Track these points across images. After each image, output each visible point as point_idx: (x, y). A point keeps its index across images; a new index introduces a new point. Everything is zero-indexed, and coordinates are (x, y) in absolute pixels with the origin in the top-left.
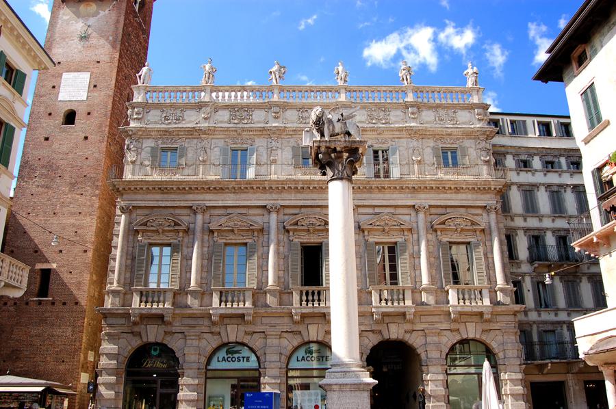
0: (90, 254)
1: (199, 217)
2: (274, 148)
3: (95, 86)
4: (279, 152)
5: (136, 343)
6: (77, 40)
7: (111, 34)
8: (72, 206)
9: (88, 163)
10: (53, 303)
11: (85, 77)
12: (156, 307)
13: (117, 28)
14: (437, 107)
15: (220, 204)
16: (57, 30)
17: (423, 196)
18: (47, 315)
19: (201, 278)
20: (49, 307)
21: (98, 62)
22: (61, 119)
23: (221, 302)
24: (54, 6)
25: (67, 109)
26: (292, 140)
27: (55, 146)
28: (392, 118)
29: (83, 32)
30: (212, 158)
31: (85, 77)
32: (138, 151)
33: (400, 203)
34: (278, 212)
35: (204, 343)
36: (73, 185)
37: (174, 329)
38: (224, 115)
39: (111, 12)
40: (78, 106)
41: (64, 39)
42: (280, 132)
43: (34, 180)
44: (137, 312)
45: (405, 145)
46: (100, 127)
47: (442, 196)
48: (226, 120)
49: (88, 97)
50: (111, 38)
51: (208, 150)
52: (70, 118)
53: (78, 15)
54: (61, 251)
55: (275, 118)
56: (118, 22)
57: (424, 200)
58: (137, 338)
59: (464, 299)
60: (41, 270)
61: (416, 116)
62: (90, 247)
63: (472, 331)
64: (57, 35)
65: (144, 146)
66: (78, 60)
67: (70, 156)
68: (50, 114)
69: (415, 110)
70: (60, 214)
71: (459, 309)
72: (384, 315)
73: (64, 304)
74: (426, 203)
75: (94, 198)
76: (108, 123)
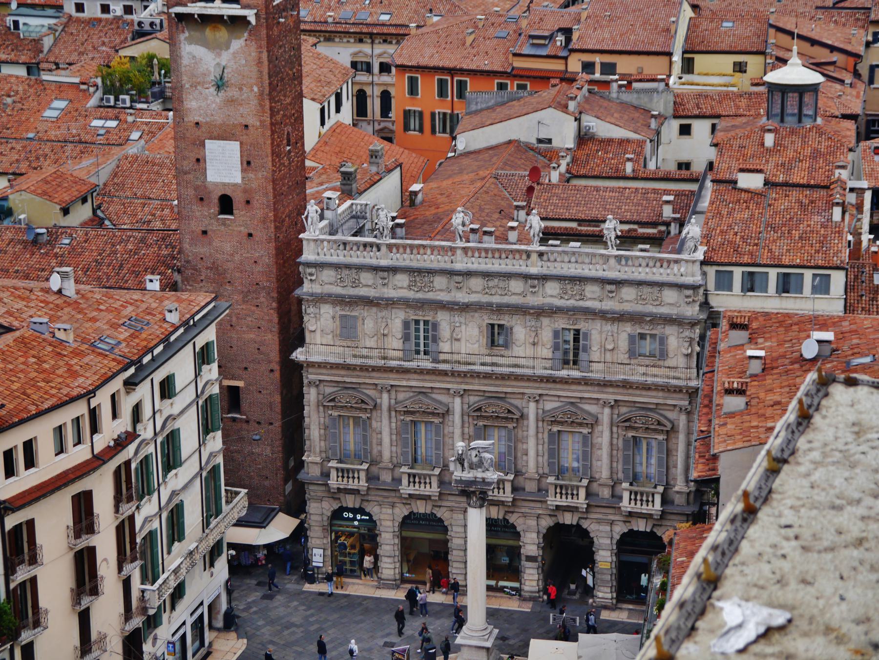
0: (277, 375)
1: (385, 396)
2: (458, 324)
3: (249, 163)
4: (463, 327)
5: (336, 506)
6: (212, 90)
7: (253, 81)
8: (250, 319)
9: (259, 268)
10: (247, 422)
11: (234, 147)
12: (352, 485)
13: (261, 72)
14: (640, 283)
15: (404, 383)
16: (183, 69)
17: (611, 390)
18: (243, 433)
19: (391, 452)
20: (245, 426)
21: (246, 126)
22: (215, 209)
23: (409, 482)
24: (176, 61)
25: (220, 194)
26: (476, 315)
27: (216, 243)
28: (587, 294)
29: (218, 77)
30: (394, 330)
31: (234, 147)
32: (317, 317)
33: (586, 395)
34: (462, 396)
35: (397, 511)
36: (245, 294)
37: (370, 498)
38: (402, 280)
39: (248, 42)
40: (234, 191)
41: (194, 86)
42: (465, 308)
43: (201, 284)
44: (335, 486)
45: (598, 327)
46: (264, 222)
47: (630, 391)
48: (405, 286)
49: (243, 178)
50: (256, 89)
51: (389, 321)
52: (226, 204)
53: (206, 44)
54: (246, 368)
55: (457, 288)
56: (259, 62)
57: (610, 396)
58: (337, 502)
59: (636, 500)
60: (229, 387)
61: (614, 295)
62: (276, 367)
63: (641, 526)
64: (185, 78)
65: (322, 311)
66: (219, 121)
67: (237, 258)
68: (202, 199)
69: (613, 287)
70: (238, 328)
71: (629, 510)
72: (558, 507)
73: (259, 423)
74: (611, 398)
75: (272, 311)
76: (272, 218)
